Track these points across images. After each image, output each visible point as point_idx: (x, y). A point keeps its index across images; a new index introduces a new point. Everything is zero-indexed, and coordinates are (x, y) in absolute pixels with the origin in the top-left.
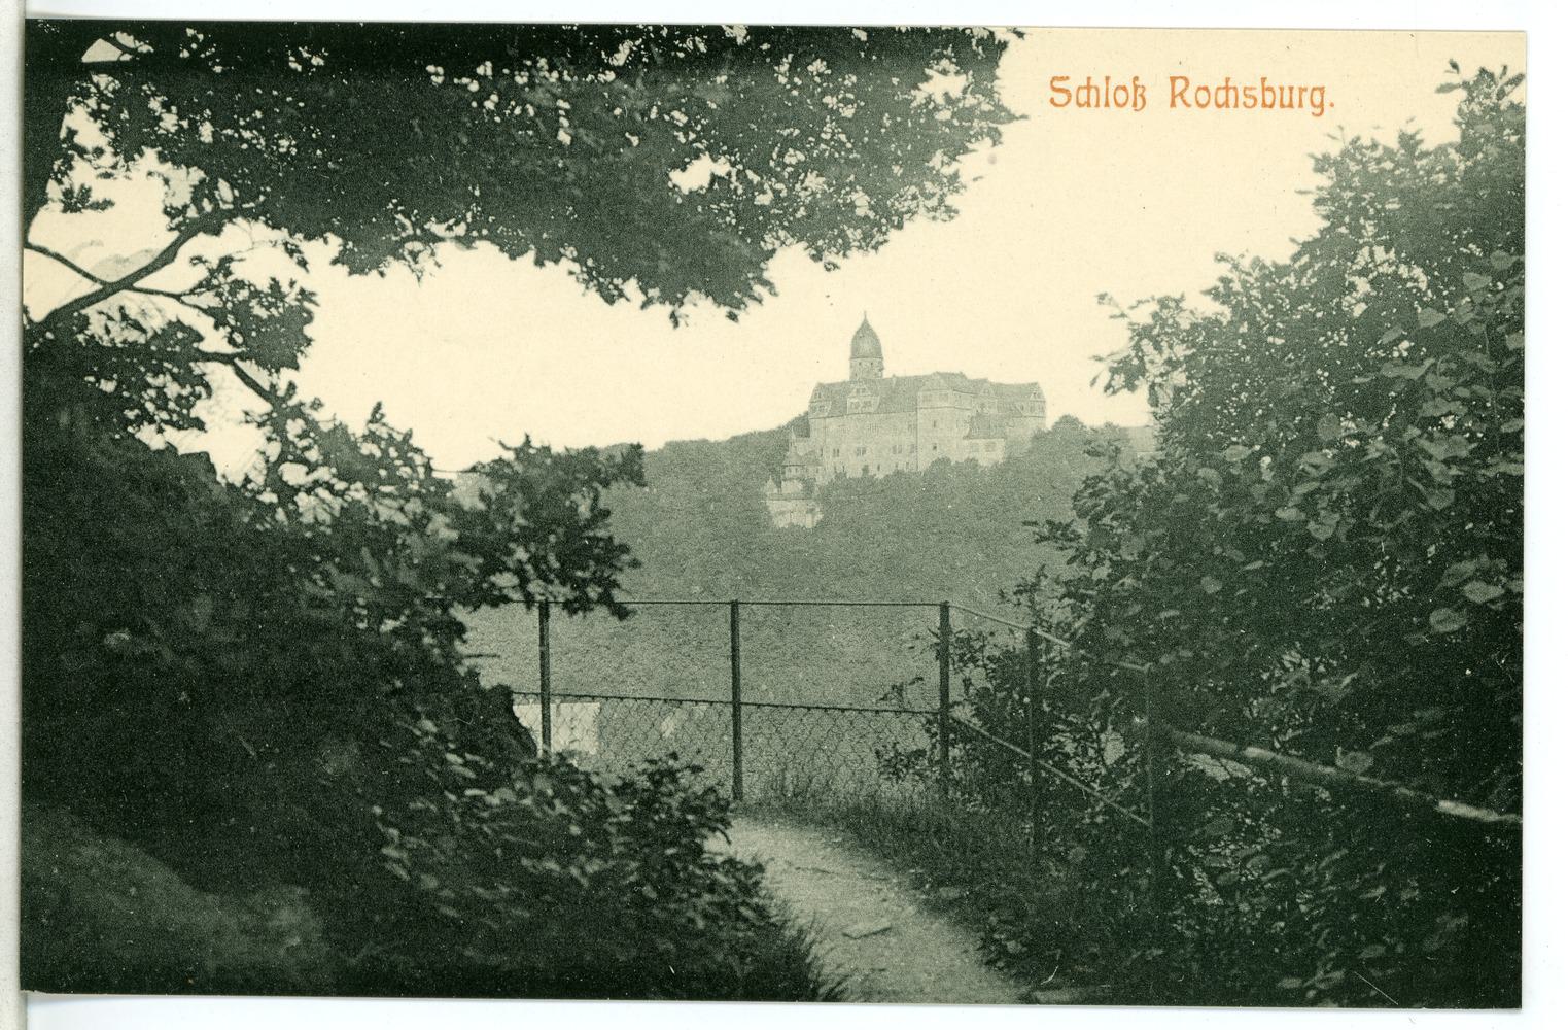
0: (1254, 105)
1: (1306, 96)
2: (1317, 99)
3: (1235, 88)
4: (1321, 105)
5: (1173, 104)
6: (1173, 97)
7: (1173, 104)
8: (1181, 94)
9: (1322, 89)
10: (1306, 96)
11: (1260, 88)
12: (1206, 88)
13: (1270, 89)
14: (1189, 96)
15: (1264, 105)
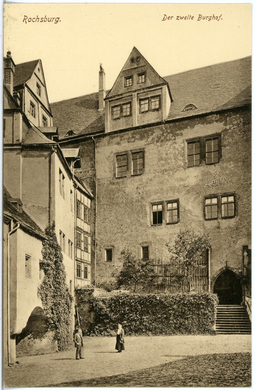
0: (43, 21)
1: (54, 19)
2: (57, 20)
3: (39, 18)
4: (57, 21)
5: (23, 21)
6: (24, 19)
7: (23, 21)
8: (26, 19)
9: (59, 18)
10: (54, 19)
11: (44, 18)
12: (31, 18)
13: (46, 18)
14: (27, 20)
15: (45, 21)
